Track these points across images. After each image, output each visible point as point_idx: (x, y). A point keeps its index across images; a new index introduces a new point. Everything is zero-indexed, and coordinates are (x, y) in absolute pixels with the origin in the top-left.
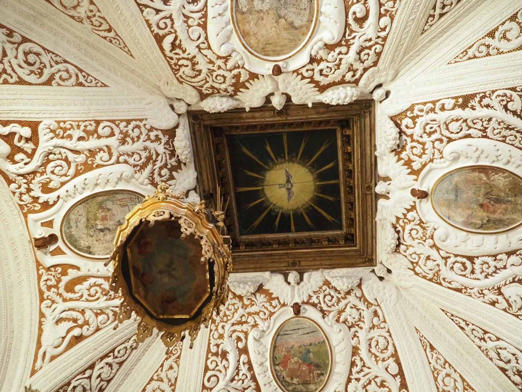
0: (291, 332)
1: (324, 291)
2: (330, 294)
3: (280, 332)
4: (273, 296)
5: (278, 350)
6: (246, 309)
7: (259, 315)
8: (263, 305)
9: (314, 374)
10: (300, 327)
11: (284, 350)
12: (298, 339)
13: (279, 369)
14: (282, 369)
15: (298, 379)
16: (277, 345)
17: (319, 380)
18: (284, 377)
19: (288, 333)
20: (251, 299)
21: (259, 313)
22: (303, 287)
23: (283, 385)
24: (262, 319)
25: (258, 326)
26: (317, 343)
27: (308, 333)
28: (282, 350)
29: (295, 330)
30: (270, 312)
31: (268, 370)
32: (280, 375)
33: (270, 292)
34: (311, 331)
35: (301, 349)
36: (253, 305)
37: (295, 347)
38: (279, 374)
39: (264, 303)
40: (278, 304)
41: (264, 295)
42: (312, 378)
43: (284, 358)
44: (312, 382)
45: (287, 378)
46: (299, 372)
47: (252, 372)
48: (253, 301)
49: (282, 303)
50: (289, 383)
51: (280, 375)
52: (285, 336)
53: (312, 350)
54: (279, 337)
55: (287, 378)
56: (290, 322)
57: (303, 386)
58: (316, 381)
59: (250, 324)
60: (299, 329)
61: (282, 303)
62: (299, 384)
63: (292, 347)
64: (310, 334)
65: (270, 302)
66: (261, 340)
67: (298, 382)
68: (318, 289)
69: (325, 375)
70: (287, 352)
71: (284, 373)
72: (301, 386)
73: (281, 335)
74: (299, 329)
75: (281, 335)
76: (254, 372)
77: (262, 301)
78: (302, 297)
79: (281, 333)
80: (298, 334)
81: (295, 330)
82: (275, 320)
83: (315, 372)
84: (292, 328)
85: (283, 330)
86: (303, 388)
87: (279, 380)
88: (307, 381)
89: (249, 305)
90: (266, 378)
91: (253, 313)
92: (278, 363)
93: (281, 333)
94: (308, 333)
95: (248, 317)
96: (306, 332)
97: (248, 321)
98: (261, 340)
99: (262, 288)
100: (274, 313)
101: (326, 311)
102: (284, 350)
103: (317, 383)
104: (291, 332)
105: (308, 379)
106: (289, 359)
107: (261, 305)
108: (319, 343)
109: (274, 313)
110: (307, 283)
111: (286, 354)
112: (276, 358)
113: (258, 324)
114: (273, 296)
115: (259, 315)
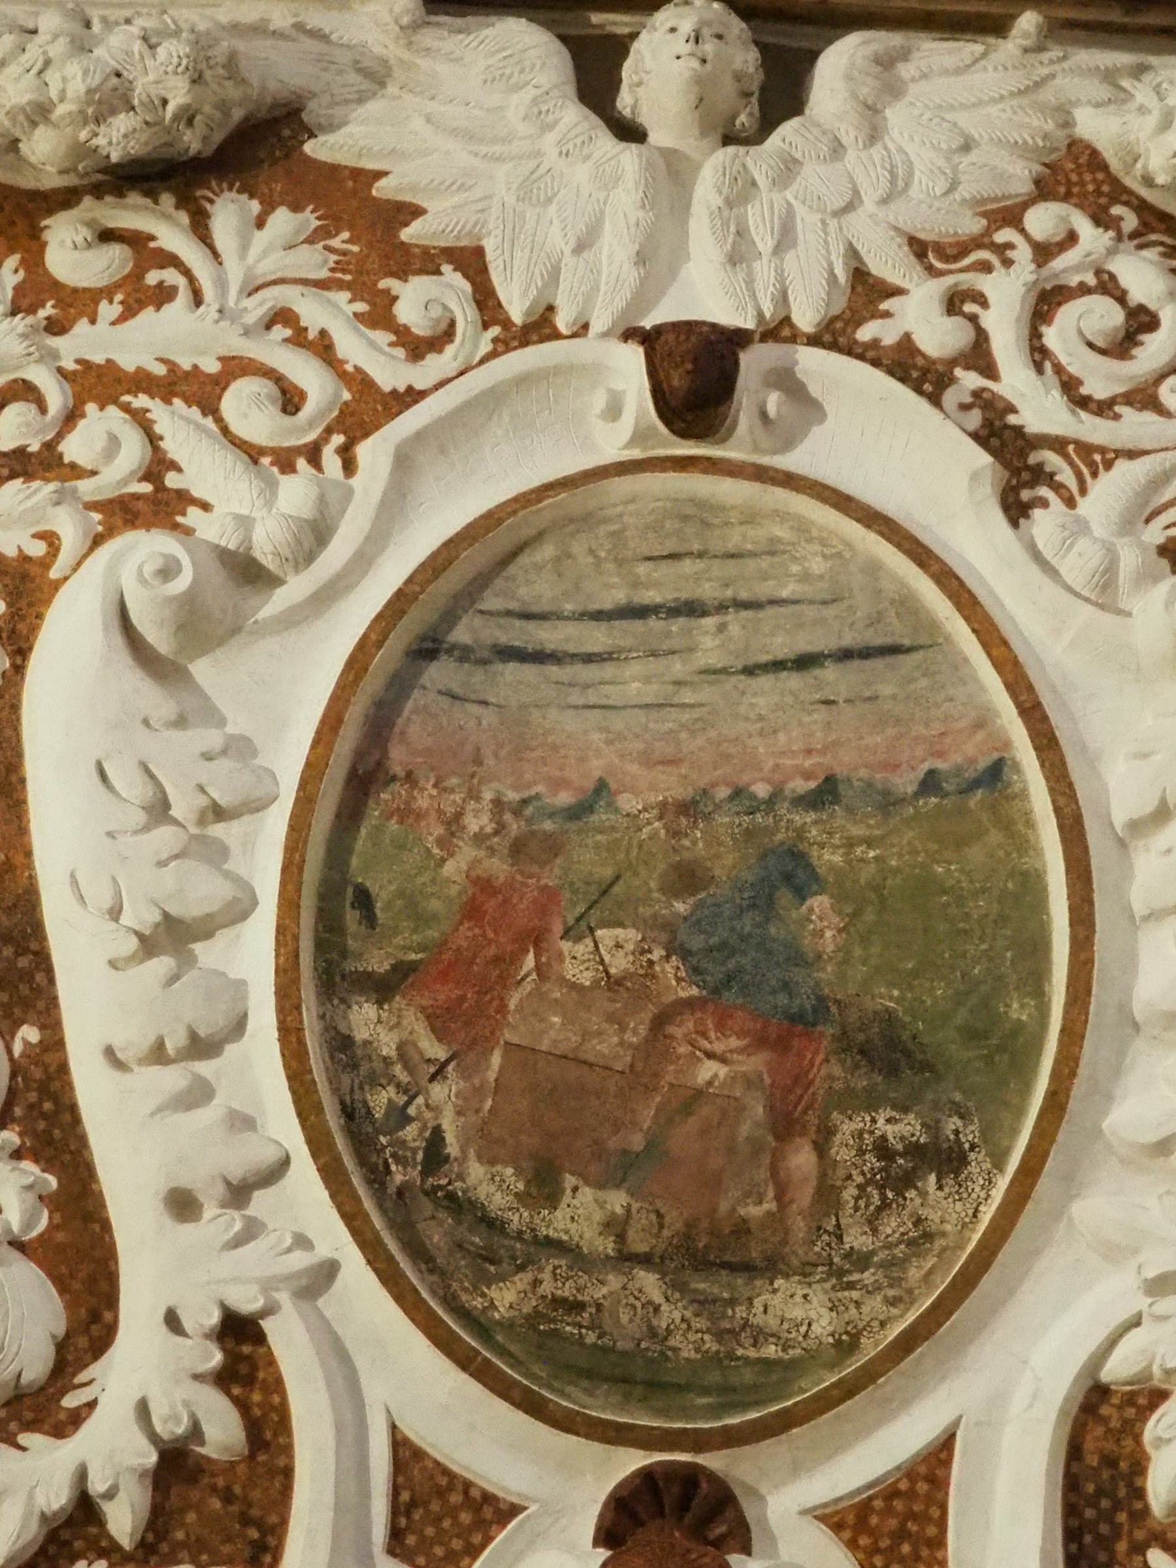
0: (598, 638)
1: (1044, 252)
2: (1108, 286)
3: (450, 617)
4: (408, 234)
5: (406, 813)
6: (56, 327)
7: (211, 409)
8: (283, 316)
9: (842, 1152)
10: (708, 591)
11: (477, 822)
12: (669, 721)
13: (387, 1045)
14: (437, 1051)
15: (617, 1201)
16: (398, 757)
17: (890, 1226)
18: (436, 1139)
19: (548, 636)
20: (136, 241)
21: (221, 382)
22: (789, 168)
23: (419, 1252)
24: (252, 453)
25: (192, 516)
26: (906, 782)
27: (805, 662)
28: (454, 822)
29: (639, 612)
30: (360, 382)
31: (238, 1027)
32: (400, 1117)
33: (382, 189)
34: (848, 640)
35: (696, 843)
36: (163, 296)
37: (628, 803)
38: (381, 1100)
39: (290, 297)
40: (465, 315)
41: (310, 219)
42: (804, 1197)
43: (472, 911)
44: (798, 1251)
45: (476, 1171)
46: (647, 1116)
47: (29, 1034)
48: (172, 261)
49: (517, 313)
50: (492, 1224)
51: (400, 1117)
52: (511, 670)
53: (829, 858)
54: (439, 673)
55: (476, 1171)
56: (586, 521)
57: (677, 1286)
58: (857, 1239)
59: (85, 487)
60: (692, 609)
61: (517, 313)
62: (627, 1259)
63: (578, 812)
64: (830, 673)
65: (359, 290)
66: (201, 669)
67: (616, 1227)
68: (973, 225)
69: (978, 1162)
70: (518, 849)
71: (438, 1091)
72: (649, 1282)
73: (464, 654)
74: (692, 609)
75: (464, 654)
76: (54, 1042)
77: (268, 268)
78: (764, 272)
79: (460, 634)
80: (678, 668)
81: (639, 612)
82: (403, 461)
83: (847, 1127)
84: (618, 596)
85: (491, 601)
86: (671, 1314)
87: (377, 1177)
88: (742, 1229)
89: (107, 293)
90: (209, 1115)
91: (142, 382)
92: (378, 962)
93: (460, 634)
94: (805, 662)
95: (72, 417)
96: (782, 646)
97: (73, 449)
98: (201, 669)
99: (292, 149)
100: (412, 396)
101: (1059, 444)
102: (477, 822)
103: (862, 1261)
104: (598, 638)
105: (754, 1211)
106: (537, 939)
107: (257, 308)
108: (930, 783)
109: (412, 396)
110: (849, 134)
111: (499, 868)
112: (364, 900)
113: (184, 498)
114: (408, 234)
115: (211, 409)
